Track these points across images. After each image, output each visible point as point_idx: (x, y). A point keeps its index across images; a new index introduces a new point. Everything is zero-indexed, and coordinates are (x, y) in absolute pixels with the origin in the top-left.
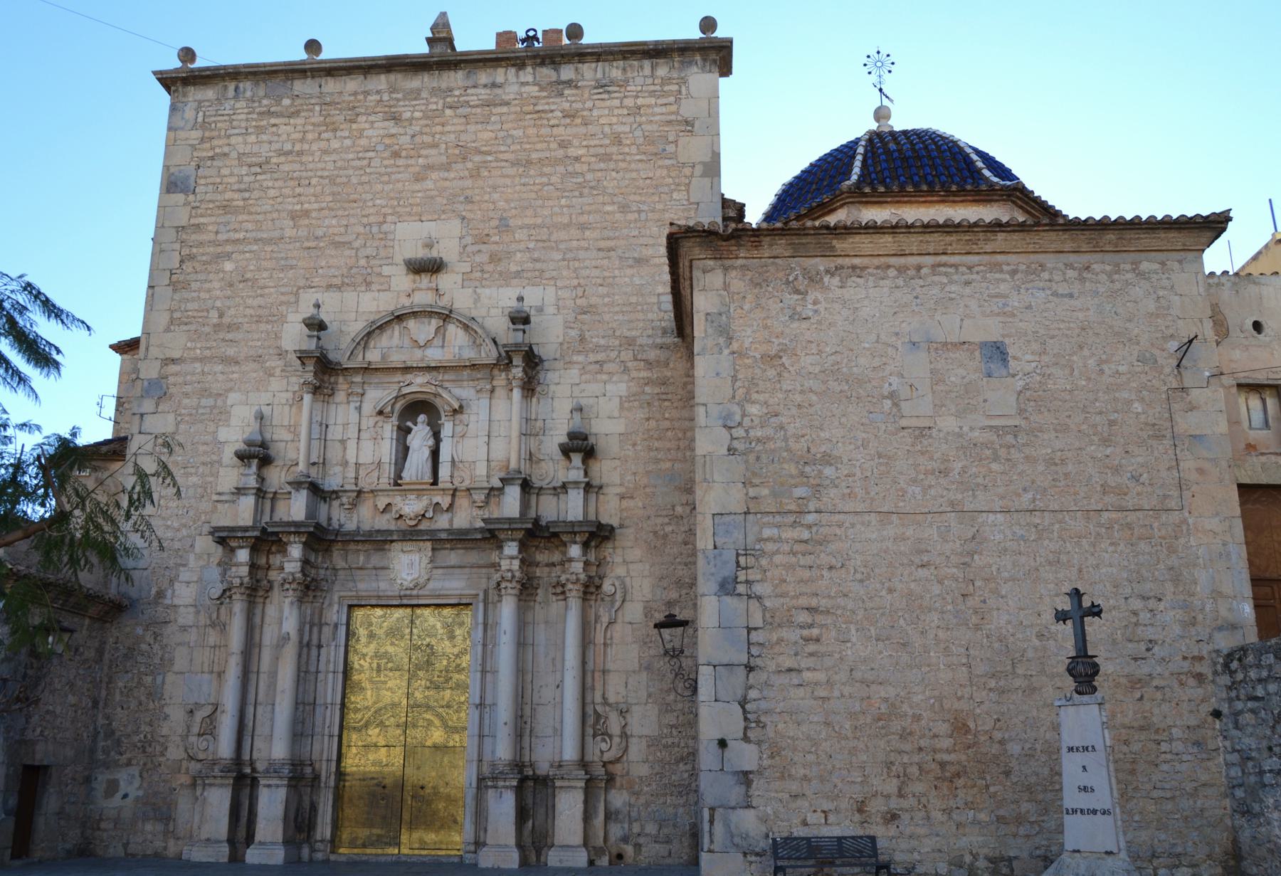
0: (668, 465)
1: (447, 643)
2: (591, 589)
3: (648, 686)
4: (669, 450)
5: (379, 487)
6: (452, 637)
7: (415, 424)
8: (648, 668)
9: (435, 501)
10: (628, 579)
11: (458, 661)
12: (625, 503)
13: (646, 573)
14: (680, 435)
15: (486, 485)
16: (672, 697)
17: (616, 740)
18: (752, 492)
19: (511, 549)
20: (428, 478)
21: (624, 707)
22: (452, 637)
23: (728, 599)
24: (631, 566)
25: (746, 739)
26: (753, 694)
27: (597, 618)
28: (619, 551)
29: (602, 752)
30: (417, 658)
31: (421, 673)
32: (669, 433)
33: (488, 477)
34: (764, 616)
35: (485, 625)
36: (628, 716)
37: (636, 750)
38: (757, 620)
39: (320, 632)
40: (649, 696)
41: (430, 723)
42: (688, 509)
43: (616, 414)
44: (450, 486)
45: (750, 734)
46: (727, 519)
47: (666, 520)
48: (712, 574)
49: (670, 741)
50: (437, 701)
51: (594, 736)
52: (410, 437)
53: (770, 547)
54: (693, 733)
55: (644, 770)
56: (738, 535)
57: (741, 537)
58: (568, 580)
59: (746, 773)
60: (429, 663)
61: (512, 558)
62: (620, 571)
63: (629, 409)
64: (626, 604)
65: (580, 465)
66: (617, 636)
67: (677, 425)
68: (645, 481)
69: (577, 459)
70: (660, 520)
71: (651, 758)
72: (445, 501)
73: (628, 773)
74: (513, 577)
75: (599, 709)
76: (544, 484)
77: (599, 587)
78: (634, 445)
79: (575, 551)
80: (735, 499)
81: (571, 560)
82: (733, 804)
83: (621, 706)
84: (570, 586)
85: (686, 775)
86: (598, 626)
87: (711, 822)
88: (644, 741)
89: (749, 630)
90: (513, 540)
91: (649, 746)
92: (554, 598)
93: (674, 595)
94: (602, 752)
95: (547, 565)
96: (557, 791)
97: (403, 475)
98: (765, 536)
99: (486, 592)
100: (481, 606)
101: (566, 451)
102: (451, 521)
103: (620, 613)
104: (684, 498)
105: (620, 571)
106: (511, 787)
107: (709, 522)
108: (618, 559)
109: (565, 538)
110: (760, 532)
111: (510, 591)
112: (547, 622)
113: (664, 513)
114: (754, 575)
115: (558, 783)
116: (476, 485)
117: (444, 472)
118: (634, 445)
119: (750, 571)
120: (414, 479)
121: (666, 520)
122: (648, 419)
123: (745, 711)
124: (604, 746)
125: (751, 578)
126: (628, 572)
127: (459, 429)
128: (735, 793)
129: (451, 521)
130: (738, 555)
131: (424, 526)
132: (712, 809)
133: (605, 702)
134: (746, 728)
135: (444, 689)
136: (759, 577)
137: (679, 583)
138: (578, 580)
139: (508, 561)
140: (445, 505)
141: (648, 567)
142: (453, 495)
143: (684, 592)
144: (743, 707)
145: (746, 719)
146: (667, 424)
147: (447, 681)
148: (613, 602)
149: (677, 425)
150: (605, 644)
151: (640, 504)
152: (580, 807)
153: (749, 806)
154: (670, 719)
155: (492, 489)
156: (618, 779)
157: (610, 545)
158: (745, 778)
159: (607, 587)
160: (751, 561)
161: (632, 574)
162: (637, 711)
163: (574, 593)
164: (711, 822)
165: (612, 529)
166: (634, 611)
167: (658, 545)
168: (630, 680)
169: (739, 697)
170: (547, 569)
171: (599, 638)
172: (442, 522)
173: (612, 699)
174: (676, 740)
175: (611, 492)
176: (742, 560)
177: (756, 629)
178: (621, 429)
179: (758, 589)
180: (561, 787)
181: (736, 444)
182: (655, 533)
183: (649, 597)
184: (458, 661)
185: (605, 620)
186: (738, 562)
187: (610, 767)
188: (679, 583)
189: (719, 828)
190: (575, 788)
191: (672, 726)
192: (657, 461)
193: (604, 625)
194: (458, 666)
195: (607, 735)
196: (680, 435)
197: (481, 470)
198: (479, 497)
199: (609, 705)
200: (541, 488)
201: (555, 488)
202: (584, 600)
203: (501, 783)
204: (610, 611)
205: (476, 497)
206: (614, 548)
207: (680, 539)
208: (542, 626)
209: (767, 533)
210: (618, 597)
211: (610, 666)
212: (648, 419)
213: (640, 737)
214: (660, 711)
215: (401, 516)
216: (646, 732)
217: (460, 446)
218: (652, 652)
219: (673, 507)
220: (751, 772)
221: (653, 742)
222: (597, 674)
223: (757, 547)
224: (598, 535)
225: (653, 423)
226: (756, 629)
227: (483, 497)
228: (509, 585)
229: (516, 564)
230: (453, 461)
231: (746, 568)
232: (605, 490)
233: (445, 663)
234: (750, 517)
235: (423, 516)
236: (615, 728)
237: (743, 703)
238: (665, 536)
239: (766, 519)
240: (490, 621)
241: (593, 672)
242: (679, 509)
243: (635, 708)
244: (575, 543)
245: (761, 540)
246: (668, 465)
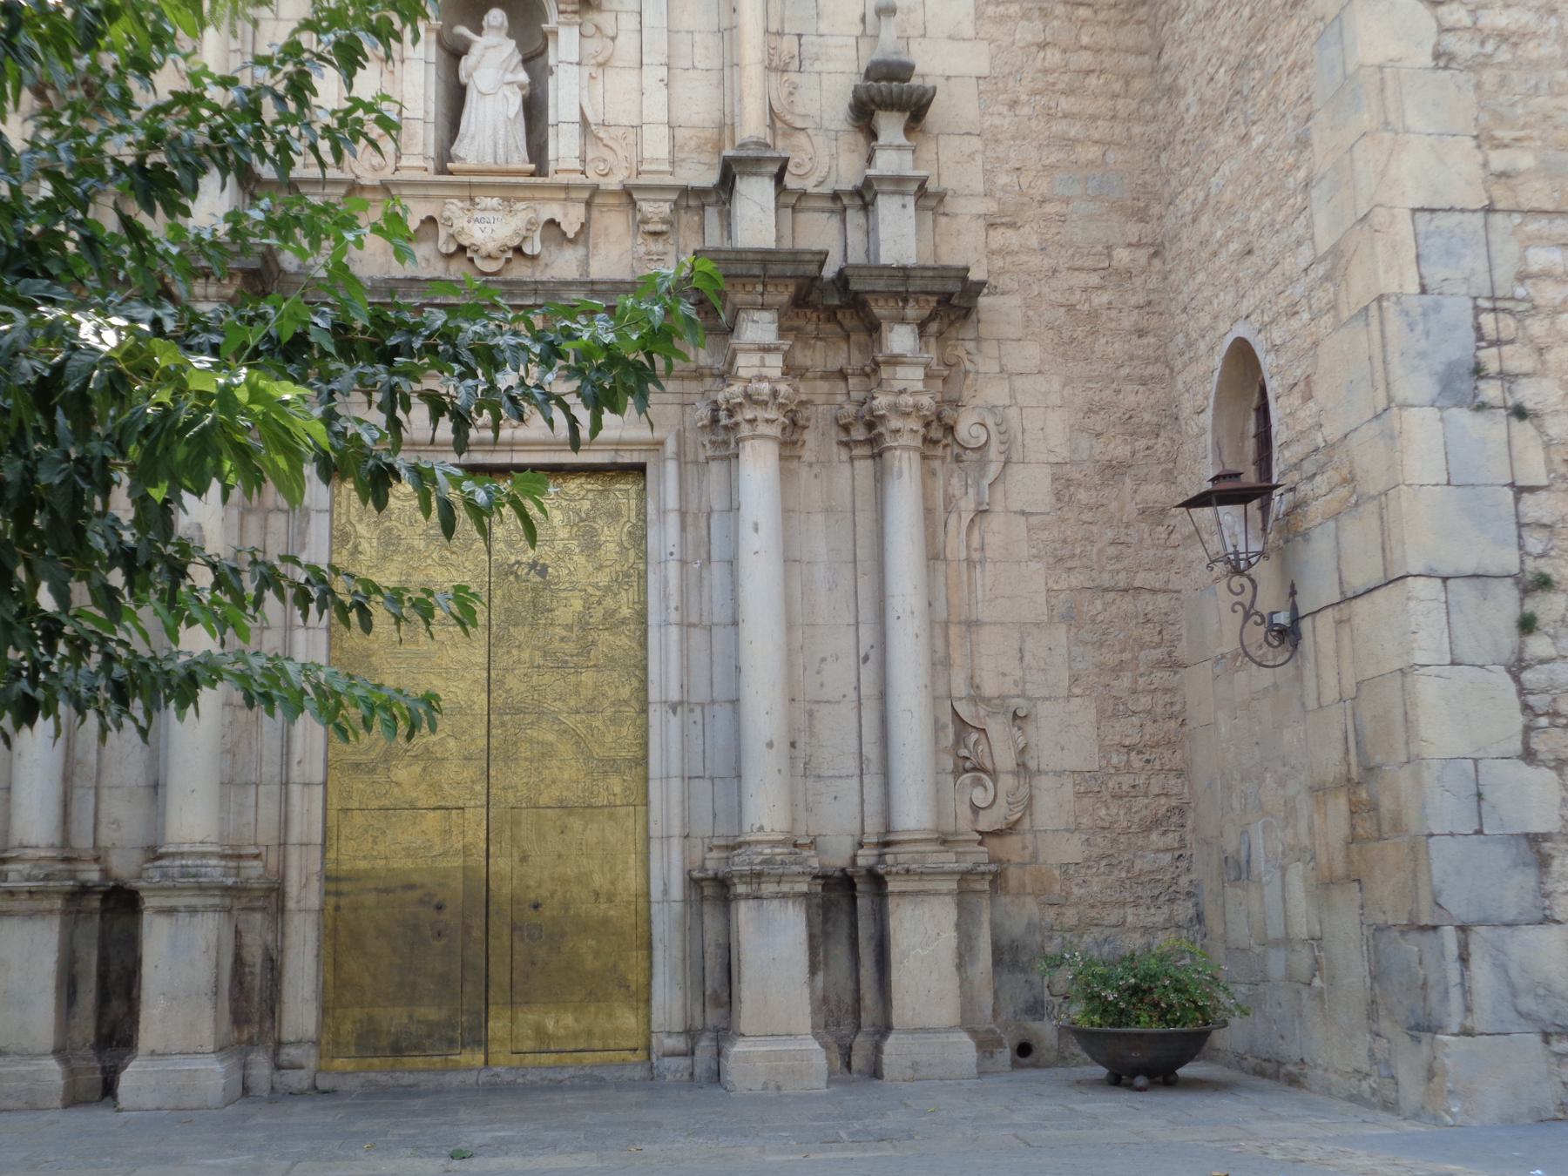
0: (1093, 152)
1: (580, 560)
2: (939, 431)
3: (1071, 659)
4: (1094, 118)
5: (404, 175)
6: (591, 546)
7: (478, 30)
8: (1070, 617)
9: (545, 216)
10: (1013, 413)
11: (609, 602)
12: (999, 238)
13: (1055, 399)
14: (1117, 87)
15: (668, 180)
16: (1126, 681)
17: (1006, 782)
18: (1499, 160)
19: (759, 328)
20: (519, 159)
21: (1023, 706)
22: (591, 546)
23: (1463, 416)
24: (1019, 383)
25: (1528, 755)
26: (1538, 646)
27: (949, 500)
28: (990, 348)
29: (975, 809)
30: (508, 597)
31: (520, 633)
32: (1092, 81)
33: (673, 163)
34: (1549, 461)
35: (683, 514)
36: (1030, 728)
37: (1053, 805)
38: (1534, 469)
39: (264, 527)
40: (1075, 679)
41: (548, 752)
42: (1142, 255)
43: (968, 31)
44: (577, 179)
45: (1537, 743)
46: (1444, 221)
47: (1094, 279)
48: (1423, 355)
49: (1127, 781)
50: (561, 698)
51: (958, 772)
52: (466, 63)
53: (1550, 293)
54: (1177, 760)
55: (1072, 849)
56: (1474, 261)
57: (1482, 266)
58: (894, 407)
59: (1534, 839)
60: (538, 608)
61: (765, 349)
62: (995, 393)
63: (1001, 19)
64: (1014, 469)
65: (901, 139)
66: (994, 541)
67: (1109, 62)
68: (1042, 187)
69: (890, 126)
70: (1080, 279)
71: (1086, 821)
72: (571, 217)
73: (1035, 857)
74: (775, 394)
75: (965, 710)
76: (809, 185)
77: (950, 429)
78: (1013, 104)
79: (900, 339)
80: (1460, 175)
81: (895, 361)
82: (1511, 914)
83: (1014, 703)
84: (895, 423)
85: (1168, 857)
86: (953, 519)
87: (1464, 959)
88: (1068, 783)
89: (1520, 491)
90: (764, 307)
91: (1079, 795)
92: (844, 454)
93: (1119, 450)
94: (975, 809)
95: (826, 376)
96: (892, 903)
97: (459, 148)
98: (1535, 268)
99: (680, 437)
100: (671, 468)
101: (864, 113)
102: (585, 263)
103: (999, 489)
104: (1134, 230)
105: (995, 393)
106: (797, 895)
107: (1404, 228)
108: (987, 365)
109: (879, 309)
110: (1523, 259)
111: (762, 429)
112: (828, 510)
113: (1089, 263)
114: (1518, 359)
115: (893, 886)
116: (645, 180)
117: (563, 147)
118: (1013, 104)
119: (1506, 349)
120: (488, 162)
121: (1094, 279)
122: (1042, 46)
123: (1522, 691)
124: (980, 797)
125: (1512, 366)
126: (1012, 396)
127: (593, 45)
128: (1514, 889)
129: (585, 263)
130: (1478, 310)
131: (520, 271)
132: (1463, 929)
133: (976, 698)
134: (1528, 730)
135: (577, 670)
136: (1528, 364)
137: (1129, 425)
138: (917, 408)
139: (755, 359)
140: (571, 229)
141: (1056, 386)
142: (589, 204)
143: (1141, 444)
144: (1516, 679)
145: (1526, 708)
146: (1084, 59)
147: (586, 648)
148: (982, 464)
149: (1109, 62)
150: (970, 562)
151: (1034, 242)
152: (949, 937)
153: (1547, 920)
154: (1127, 731)
155: (686, 191)
156: (1013, 874)
157: (968, 332)
158: (1536, 850)
159: (967, 428)
160: (1508, 326)
161: (1019, 397)
162: (1048, 716)
163: (906, 439)
164: (1464, 959)
165: (973, 290)
166: (1030, 486)
167: (1079, 333)
168: (1030, 645)
169: (1507, 653)
170: (824, 386)
171: (956, 545)
172: (564, 265)
173: (990, 688)
174: (1141, 781)
175: (968, 209)
176: (1487, 320)
177: (1532, 489)
178: (986, 72)
179: (1527, 393)
180: (902, 894)
181: (1450, 42)
182: (1071, 308)
183: (1063, 453)
184: (609, 602)
185: (968, 505)
186: (1478, 328)
187: (994, 842)
188: (1129, 425)
189: (1482, 972)
190: (937, 893)
191: (1130, 748)
192: (1070, 143)
193: (967, 517)
194: (609, 614)
195: (979, 770)
196: (1117, 87)
197: (656, 146)
198: (656, 209)
199: (987, 701)
200: (803, 194)
201: (836, 196)
202: (924, 457)
203: (768, 888)
204: (977, 484)
205: (647, 208)
206: (978, 340)
207: (1127, 322)
208: (819, 518)
209: (1541, 258)
210: (994, 451)
211: (984, 612)
212: (1042, 46)
213: (1059, 774)
214: (1101, 712)
215: (462, 249)
216: (1072, 761)
217: (598, 88)
218: (1076, 580)
219: (1109, 248)
220: (1546, 837)
221: (1089, 786)
222: (954, 631)
223: (1520, 292)
224: (951, 302)
225: (1053, 57)
226: (1532, 489)
227: (666, 208)
228: (760, 413)
229: (775, 363)
230: (584, 122)
231: (1498, 343)
232: (950, 205)
233: (578, 605)
234: (1497, 219)
235: (518, 250)
236: (1004, 759)
237: (1517, 667)
238: (1093, 315)
239: (1534, 226)
240: (693, 507)
241: (947, 623)
242: (1122, 256)
243: (1043, 709)
244: (903, 320)
245: (1522, 277)
246: (1093, 152)
